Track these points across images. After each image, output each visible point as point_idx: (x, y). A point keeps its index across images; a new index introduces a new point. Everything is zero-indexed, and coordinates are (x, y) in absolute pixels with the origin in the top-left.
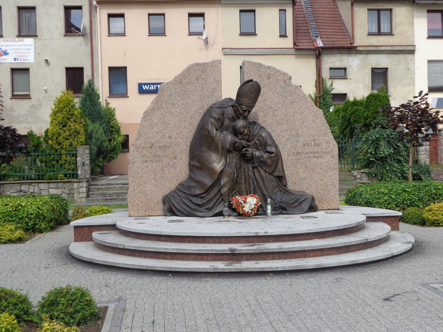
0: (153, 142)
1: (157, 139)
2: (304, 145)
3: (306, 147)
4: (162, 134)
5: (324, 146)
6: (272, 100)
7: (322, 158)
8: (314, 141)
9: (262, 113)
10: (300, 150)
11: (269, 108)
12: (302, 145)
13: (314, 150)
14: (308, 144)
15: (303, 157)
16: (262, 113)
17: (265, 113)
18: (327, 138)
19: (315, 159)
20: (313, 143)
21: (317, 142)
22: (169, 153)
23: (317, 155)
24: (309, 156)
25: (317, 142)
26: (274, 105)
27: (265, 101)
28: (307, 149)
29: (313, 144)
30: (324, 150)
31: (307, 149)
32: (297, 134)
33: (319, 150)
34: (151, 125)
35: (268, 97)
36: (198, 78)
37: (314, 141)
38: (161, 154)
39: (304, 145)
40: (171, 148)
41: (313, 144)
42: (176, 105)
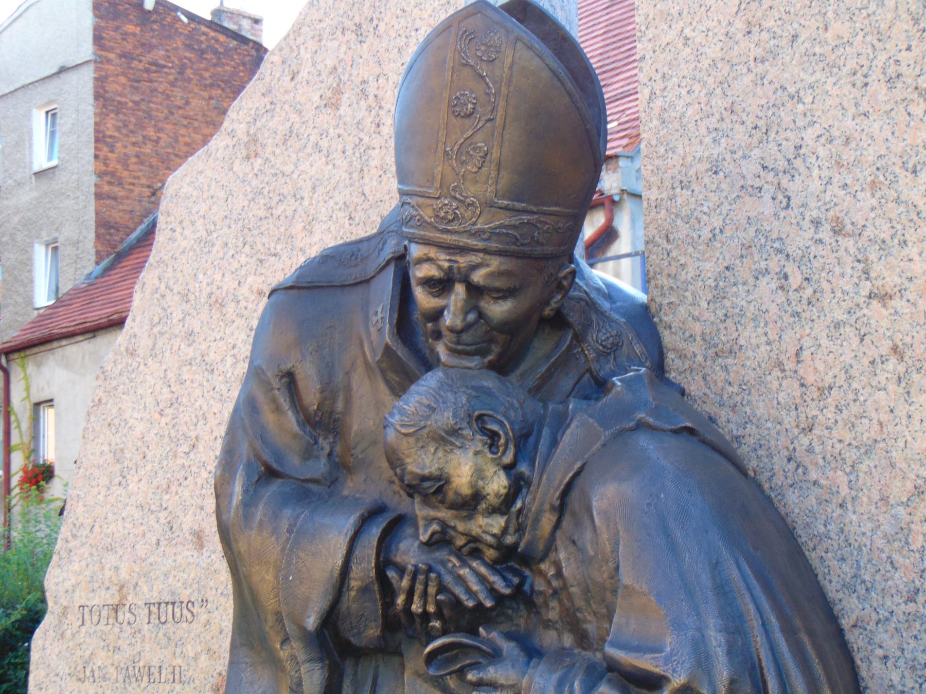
0: (124, 575)
1: (141, 550)
4: (162, 515)
6: (848, 156)
9: (767, 285)
11: (825, 234)
16: (767, 285)
17: (795, 279)
22: (190, 651)
26: (867, 200)
27: (790, 171)
34: (118, 455)
35: (809, 135)
36: (338, 92)
38: (155, 663)
40: (204, 617)
42: (230, 308)
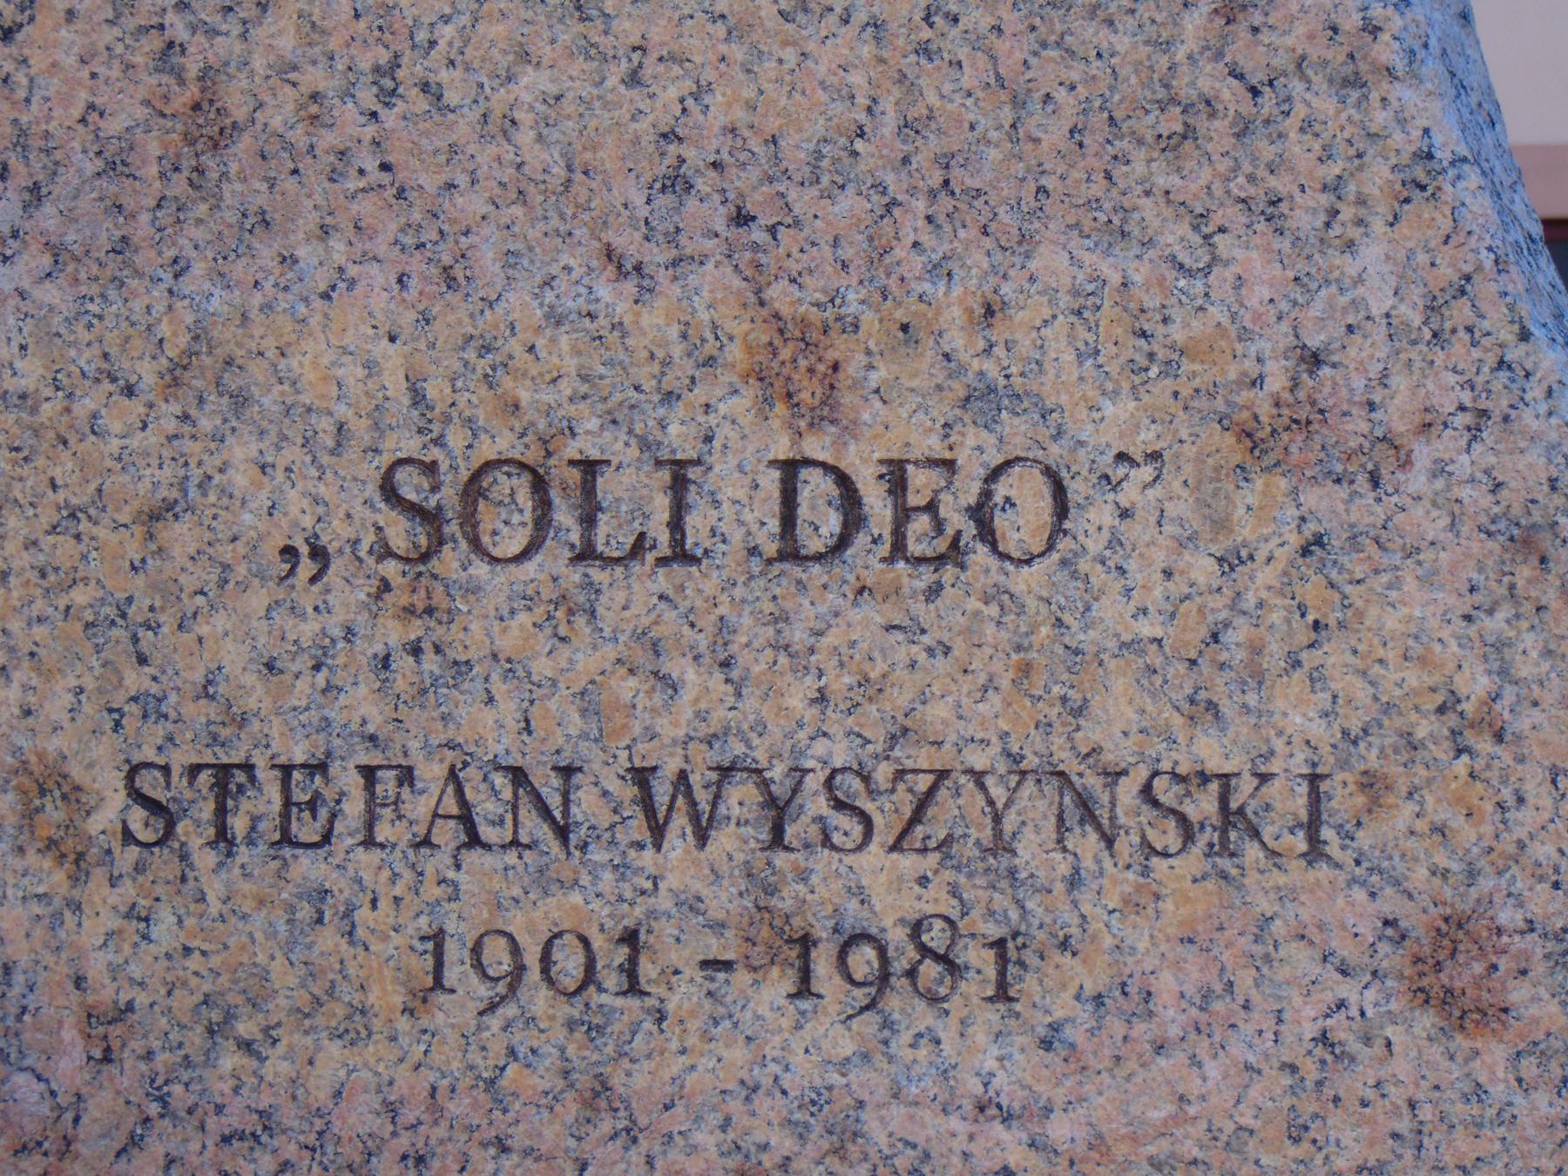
2: (435, 517)
3: (494, 601)
5: (1144, 567)
7: (1054, 992)
8: (799, 368)
10: (266, 664)
12: (353, 513)
13: (783, 720)
14: (563, 486)
15: (392, 946)
18: (1253, 260)
19: (819, 1040)
20: (744, 455)
21: (893, 417)
23: (886, 887)
24: (589, 903)
25: (893, 417)
28: (534, 662)
29: (736, 505)
30: (1119, 718)
31: (534, 662)
32: (208, 127)
33: (969, 719)
37: (799, 368)
39: (435, 517)
41: (736, 505)
